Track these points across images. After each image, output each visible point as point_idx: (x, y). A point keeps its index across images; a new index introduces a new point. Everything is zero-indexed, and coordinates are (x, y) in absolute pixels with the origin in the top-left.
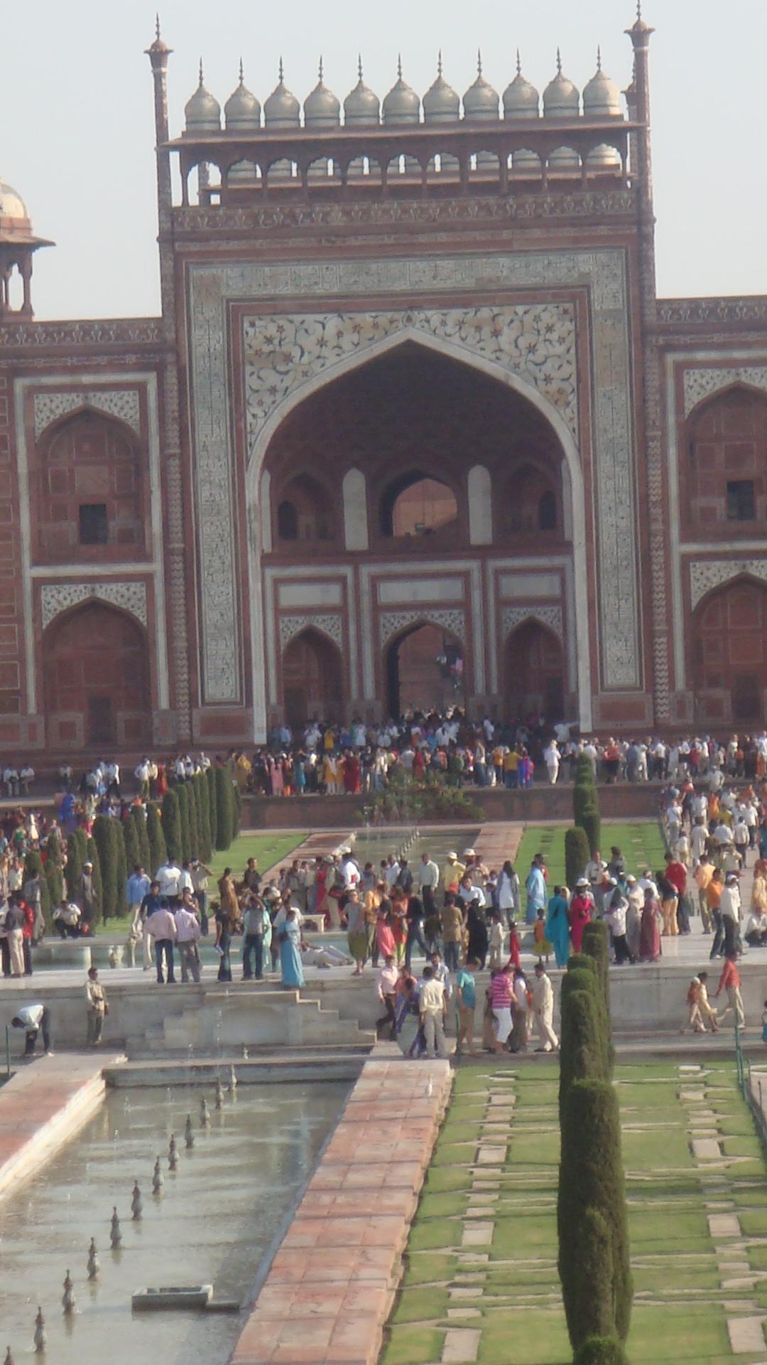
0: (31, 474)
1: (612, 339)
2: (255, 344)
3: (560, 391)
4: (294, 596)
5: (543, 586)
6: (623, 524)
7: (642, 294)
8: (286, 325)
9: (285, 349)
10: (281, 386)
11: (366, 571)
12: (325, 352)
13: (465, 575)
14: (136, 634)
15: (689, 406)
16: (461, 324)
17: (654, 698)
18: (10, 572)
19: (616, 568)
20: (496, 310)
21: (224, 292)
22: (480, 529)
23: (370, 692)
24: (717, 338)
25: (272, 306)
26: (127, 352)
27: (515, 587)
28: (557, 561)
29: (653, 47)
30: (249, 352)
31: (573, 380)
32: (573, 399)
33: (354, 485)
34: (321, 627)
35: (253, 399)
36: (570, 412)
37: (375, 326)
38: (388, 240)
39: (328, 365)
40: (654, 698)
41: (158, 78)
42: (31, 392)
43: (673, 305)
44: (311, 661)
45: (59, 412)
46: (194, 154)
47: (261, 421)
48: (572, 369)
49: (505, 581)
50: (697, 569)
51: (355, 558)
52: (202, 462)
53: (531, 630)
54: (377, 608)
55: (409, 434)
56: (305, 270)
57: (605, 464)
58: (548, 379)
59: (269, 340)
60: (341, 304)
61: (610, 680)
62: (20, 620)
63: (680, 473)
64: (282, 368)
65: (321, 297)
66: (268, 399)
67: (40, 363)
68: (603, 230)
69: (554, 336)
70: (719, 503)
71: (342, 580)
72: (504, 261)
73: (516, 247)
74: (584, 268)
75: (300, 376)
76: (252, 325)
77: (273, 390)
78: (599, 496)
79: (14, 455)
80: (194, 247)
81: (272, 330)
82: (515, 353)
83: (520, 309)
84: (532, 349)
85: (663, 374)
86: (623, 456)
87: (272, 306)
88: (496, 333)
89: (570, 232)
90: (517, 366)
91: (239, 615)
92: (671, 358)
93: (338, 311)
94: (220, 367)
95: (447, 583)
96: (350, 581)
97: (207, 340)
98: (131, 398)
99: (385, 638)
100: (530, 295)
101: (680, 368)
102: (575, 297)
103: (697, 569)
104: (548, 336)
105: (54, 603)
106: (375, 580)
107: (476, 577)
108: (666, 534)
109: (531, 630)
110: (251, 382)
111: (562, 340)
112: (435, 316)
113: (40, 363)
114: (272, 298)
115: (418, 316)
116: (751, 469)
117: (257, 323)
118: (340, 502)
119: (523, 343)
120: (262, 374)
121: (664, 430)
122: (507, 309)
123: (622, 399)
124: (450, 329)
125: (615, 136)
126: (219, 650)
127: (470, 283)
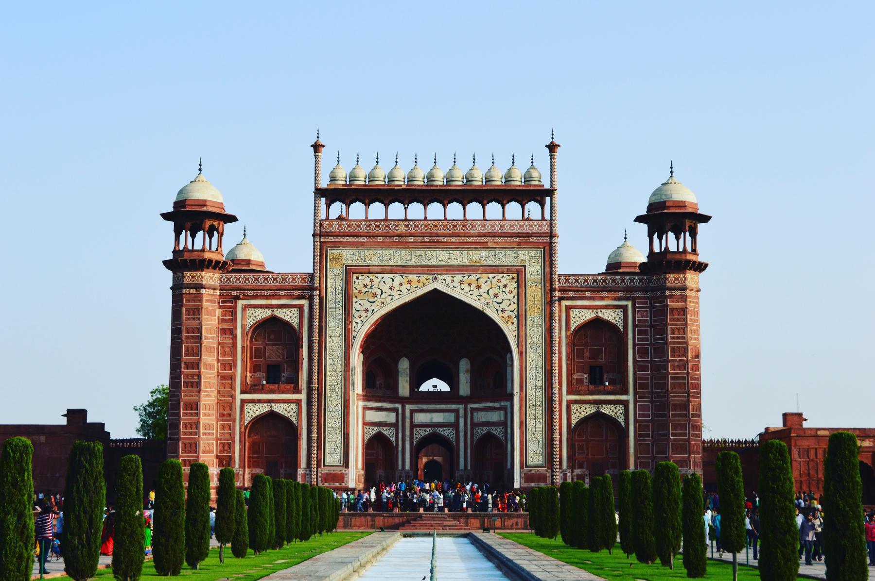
0: (243, 347)
1: (535, 292)
2: (359, 288)
3: (509, 317)
4: (373, 416)
5: (495, 417)
6: (539, 384)
7: (551, 271)
8: (375, 279)
9: (374, 291)
10: (370, 309)
11: (408, 407)
12: (393, 293)
13: (456, 411)
15: (572, 328)
16: (461, 282)
17: (552, 472)
18: (231, 396)
19: (534, 405)
20: (479, 276)
21: (344, 262)
22: (464, 389)
23: (407, 467)
24: (588, 294)
25: (367, 270)
26: (294, 290)
27: (481, 417)
28: (503, 404)
29: (559, 153)
30: (355, 291)
31: (516, 312)
32: (515, 320)
33: (404, 365)
34: (385, 433)
35: (356, 314)
36: (514, 327)
37: (419, 281)
38: (427, 239)
39: (394, 298)
40: (552, 472)
41: (316, 157)
42: (245, 308)
43: (567, 277)
44: (379, 449)
45: (259, 318)
47: (360, 326)
48: (515, 306)
49: (475, 414)
50: (574, 408)
51: (403, 401)
52: (328, 345)
53: (489, 436)
54: (413, 426)
56: (386, 253)
57: (530, 353)
58: (503, 311)
59: (366, 286)
60: (402, 270)
61: (530, 463)
62: (234, 421)
63: (567, 360)
64: (372, 300)
65: (392, 266)
66: (364, 314)
67: (251, 293)
68: (534, 240)
69: (507, 290)
70: (586, 377)
71: (396, 410)
72: (484, 253)
73: (490, 245)
74: (523, 257)
75: (380, 304)
76: (358, 278)
77: (366, 311)
79: (235, 338)
80: (332, 239)
81: (367, 281)
82: (488, 297)
83: (491, 276)
84: (496, 296)
85: (560, 311)
86: (539, 350)
87: (367, 270)
88: (478, 287)
89: (517, 240)
90: (488, 304)
92: (564, 303)
93: (401, 274)
94: (340, 298)
95: (446, 414)
96: (400, 411)
97: (334, 285)
98: (295, 311)
99: (416, 440)
100: (495, 269)
101: (568, 308)
102: (519, 273)
103: (574, 408)
104: (504, 290)
105: (251, 413)
106: (412, 412)
107: (461, 412)
108: (560, 390)
109: (489, 437)
110: (356, 306)
111: (511, 292)
112: (448, 278)
113: (251, 293)
114: (368, 266)
115: (440, 277)
116: (602, 360)
117: (360, 277)
118: (397, 372)
119: (491, 292)
120: (361, 302)
121: (560, 338)
122: (485, 276)
123: (539, 321)
124: (456, 284)
126: (333, 440)
127: (467, 263)
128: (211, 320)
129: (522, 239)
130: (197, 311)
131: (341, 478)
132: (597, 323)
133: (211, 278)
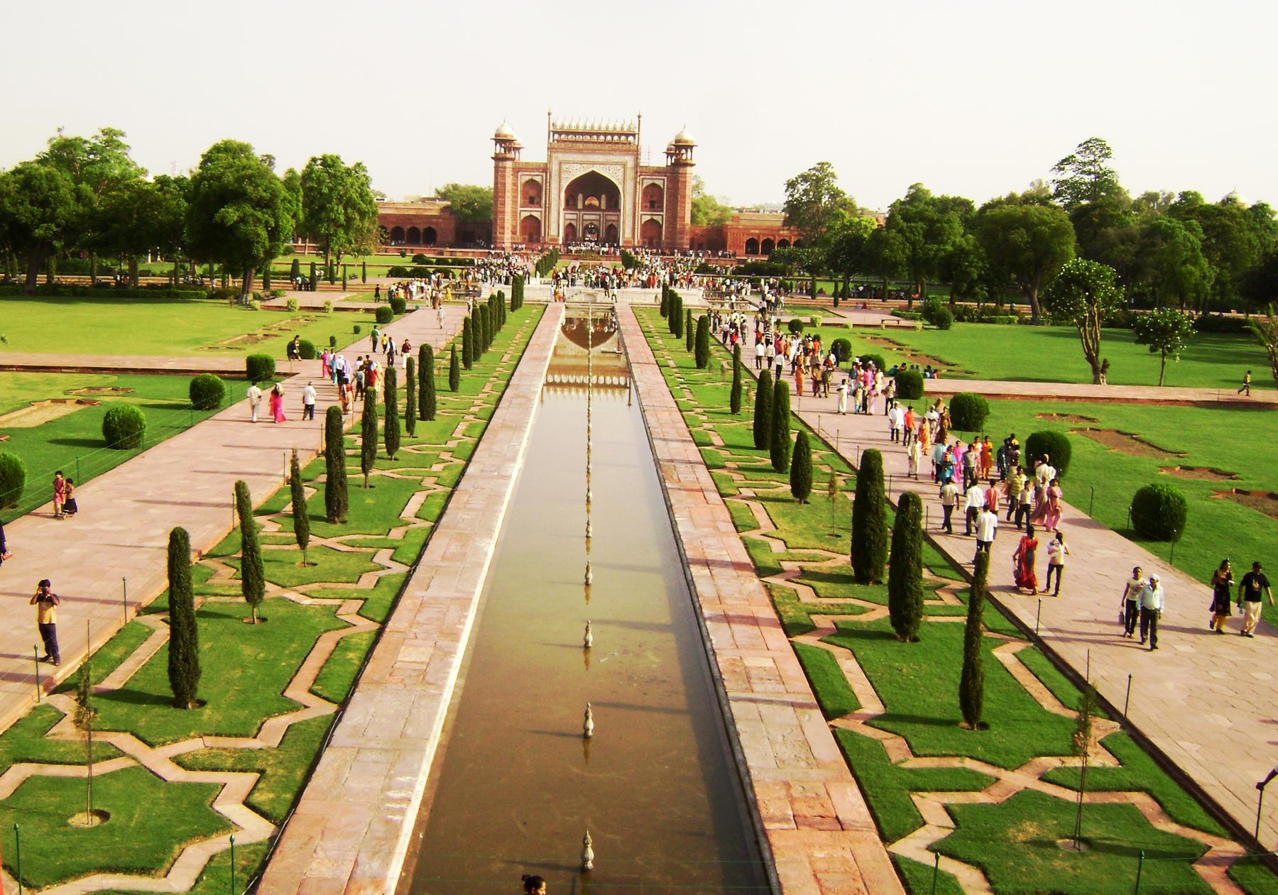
1: (630, 174)
5: (614, 218)
14: (538, 222)
22: (603, 207)
25: (568, 162)
27: (609, 218)
33: (580, 196)
44: (570, 228)
46: (555, 133)
55: (593, 188)
78: (626, 202)
87: (568, 162)
91: (557, 221)
97: (555, 168)
100: (616, 164)
102: (624, 165)
116: (655, 199)
125: (634, 135)
128: (509, 180)
129: (627, 152)
130: (504, 177)
131: (556, 240)
132: (653, 185)
133: (509, 164)
